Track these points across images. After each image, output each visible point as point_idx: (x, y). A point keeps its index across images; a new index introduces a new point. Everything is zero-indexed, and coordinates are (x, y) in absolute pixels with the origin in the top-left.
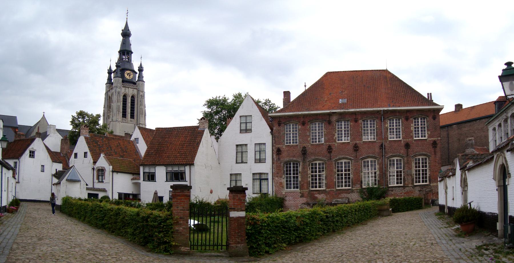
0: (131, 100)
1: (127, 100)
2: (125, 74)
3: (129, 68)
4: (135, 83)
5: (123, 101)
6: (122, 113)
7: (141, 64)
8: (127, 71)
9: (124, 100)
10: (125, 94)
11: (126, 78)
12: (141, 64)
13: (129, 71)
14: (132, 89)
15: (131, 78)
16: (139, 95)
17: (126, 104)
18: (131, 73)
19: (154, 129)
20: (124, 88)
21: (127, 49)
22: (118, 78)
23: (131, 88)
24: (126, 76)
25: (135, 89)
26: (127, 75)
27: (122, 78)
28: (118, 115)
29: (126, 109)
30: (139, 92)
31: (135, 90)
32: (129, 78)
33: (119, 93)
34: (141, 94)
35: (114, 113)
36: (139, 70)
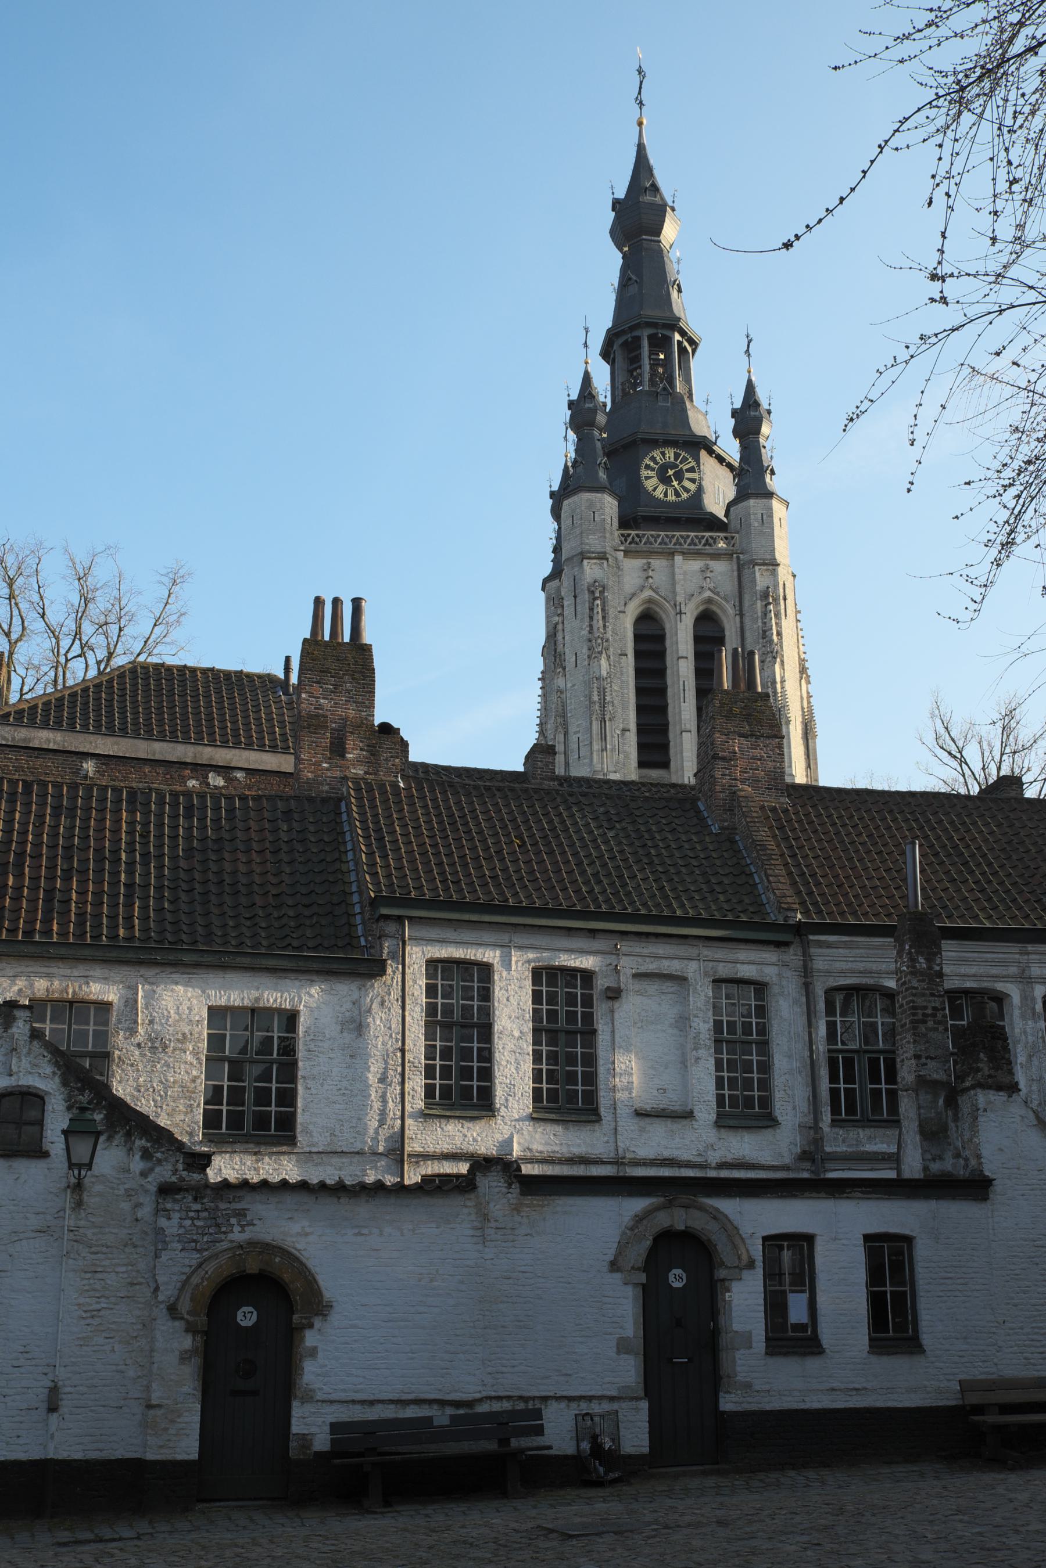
0: (698, 639)
1: (668, 643)
2: (644, 473)
3: (673, 432)
4: (712, 523)
5: (638, 654)
6: (632, 737)
7: (750, 388)
8: (656, 454)
9: (645, 647)
10: (650, 601)
11: (650, 496)
12: (750, 388)
13: (670, 453)
14: (695, 565)
15: (685, 495)
16: (747, 597)
17: (661, 673)
18: (685, 459)
19: (569, 412)
20: (638, 563)
21: (650, 312)
22: (586, 496)
23: (683, 553)
24: (651, 483)
25: (717, 556)
26: (654, 481)
27: (613, 494)
28: (596, 747)
29: (663, 709)
30: (746, 571)
31: (720, 567)
32: (671, 497)
33: (597, 591)
34: (761, 579)
35: (573, 738)
36: (736, 433)
